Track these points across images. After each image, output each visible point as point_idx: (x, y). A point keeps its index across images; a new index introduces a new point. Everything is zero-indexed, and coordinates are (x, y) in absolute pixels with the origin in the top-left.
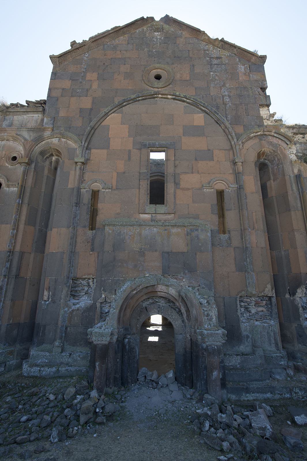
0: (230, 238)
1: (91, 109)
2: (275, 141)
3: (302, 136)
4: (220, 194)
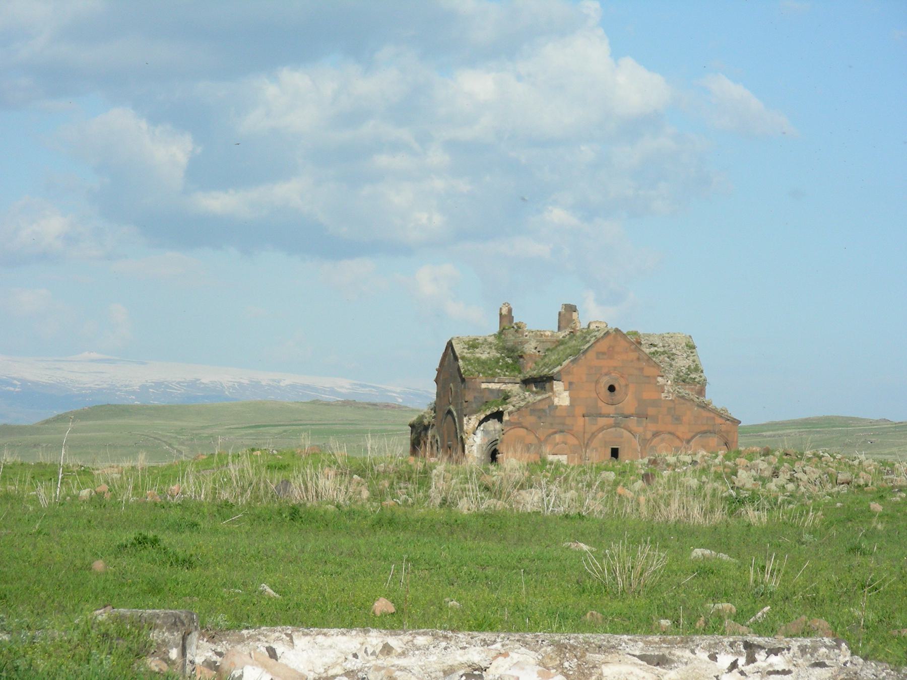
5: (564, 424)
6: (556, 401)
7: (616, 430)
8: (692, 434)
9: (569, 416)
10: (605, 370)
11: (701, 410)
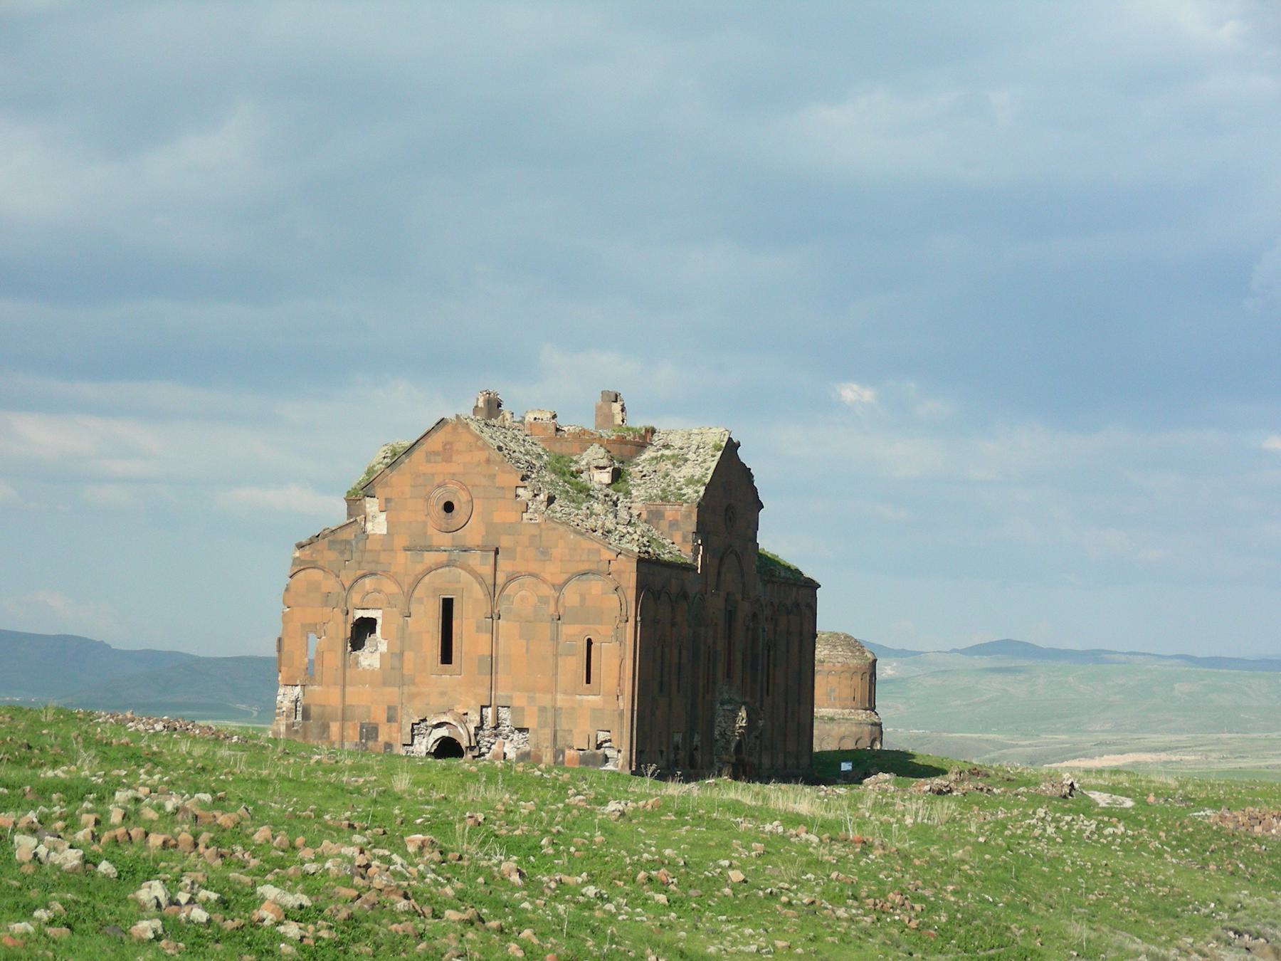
5: (377, 562)
6: (369, 526)
7: (450, 571)
8: (565, 576)
9: (384, 550)
10: (438, 480)
11: (578, 537)
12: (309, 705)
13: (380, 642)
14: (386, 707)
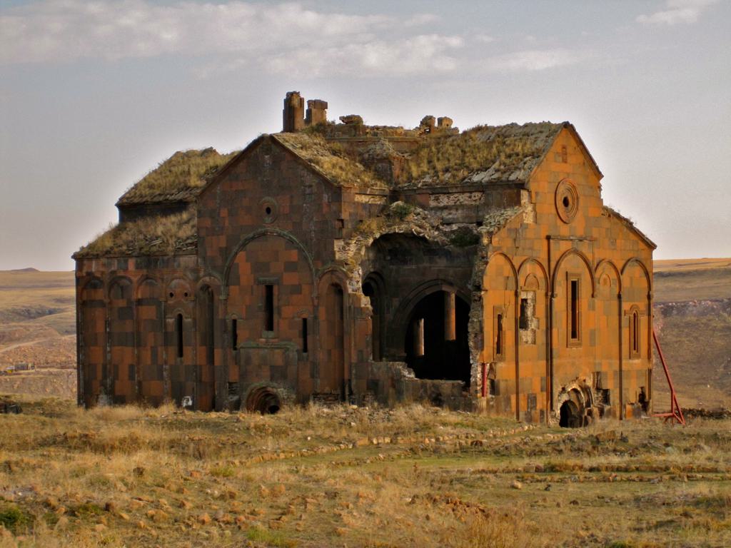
0: (308, 356)
1: (226, 248)
2: (340, 275)
3: (468, 195)
4: (305, 320)
9: (536, 239)
11: (628, 231)
12: (499, 381)
13: (532, 320)
14: (540, 378)
